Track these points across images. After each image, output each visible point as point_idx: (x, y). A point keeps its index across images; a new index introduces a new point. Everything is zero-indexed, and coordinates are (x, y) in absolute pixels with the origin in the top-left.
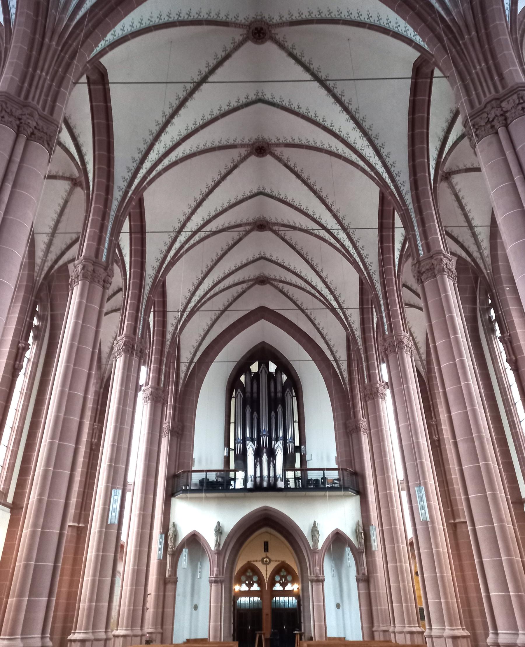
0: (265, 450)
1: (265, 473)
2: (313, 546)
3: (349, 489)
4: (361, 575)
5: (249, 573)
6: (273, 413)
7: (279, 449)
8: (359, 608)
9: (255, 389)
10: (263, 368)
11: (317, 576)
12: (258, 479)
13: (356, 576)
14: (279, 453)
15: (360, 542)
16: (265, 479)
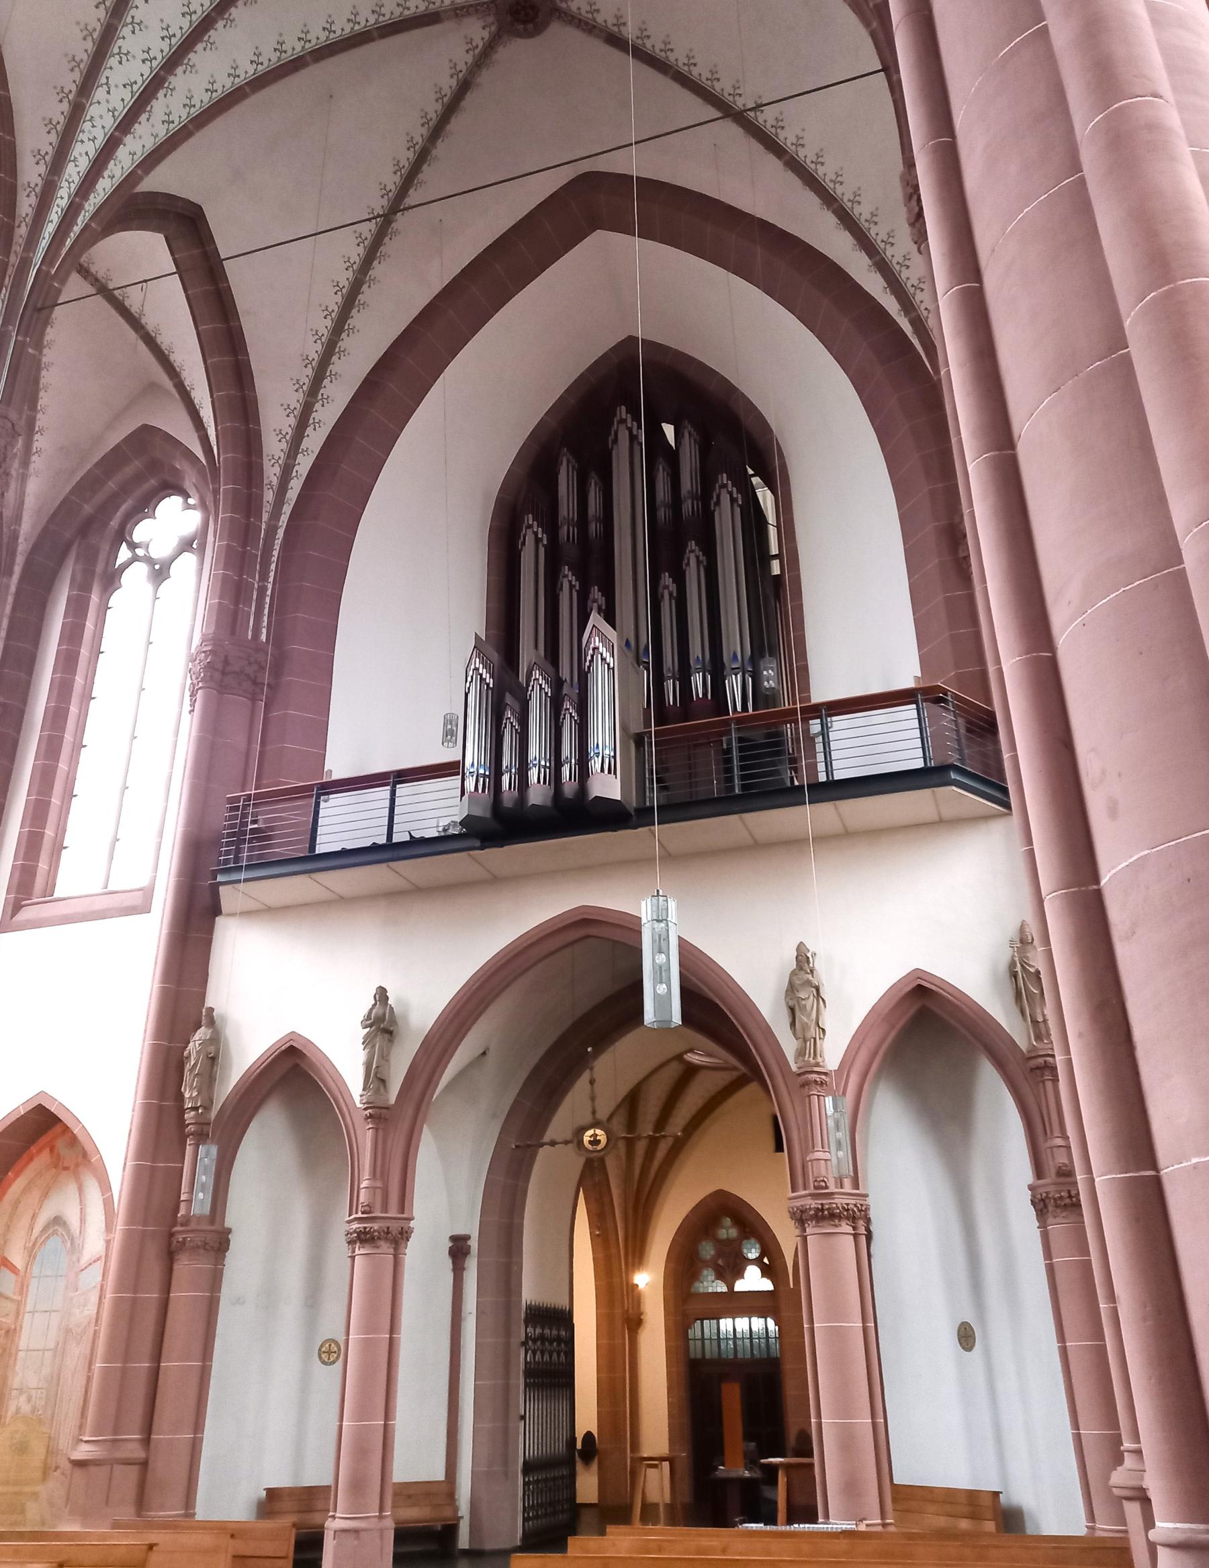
2: (801, 1053)
3: (953, 776)
4: (1051, 1177)
5: (728, 1231)
8: (1055, 1345)
11: (821, 1190)
13: (1031, 1188)
15: (1035, 1022)
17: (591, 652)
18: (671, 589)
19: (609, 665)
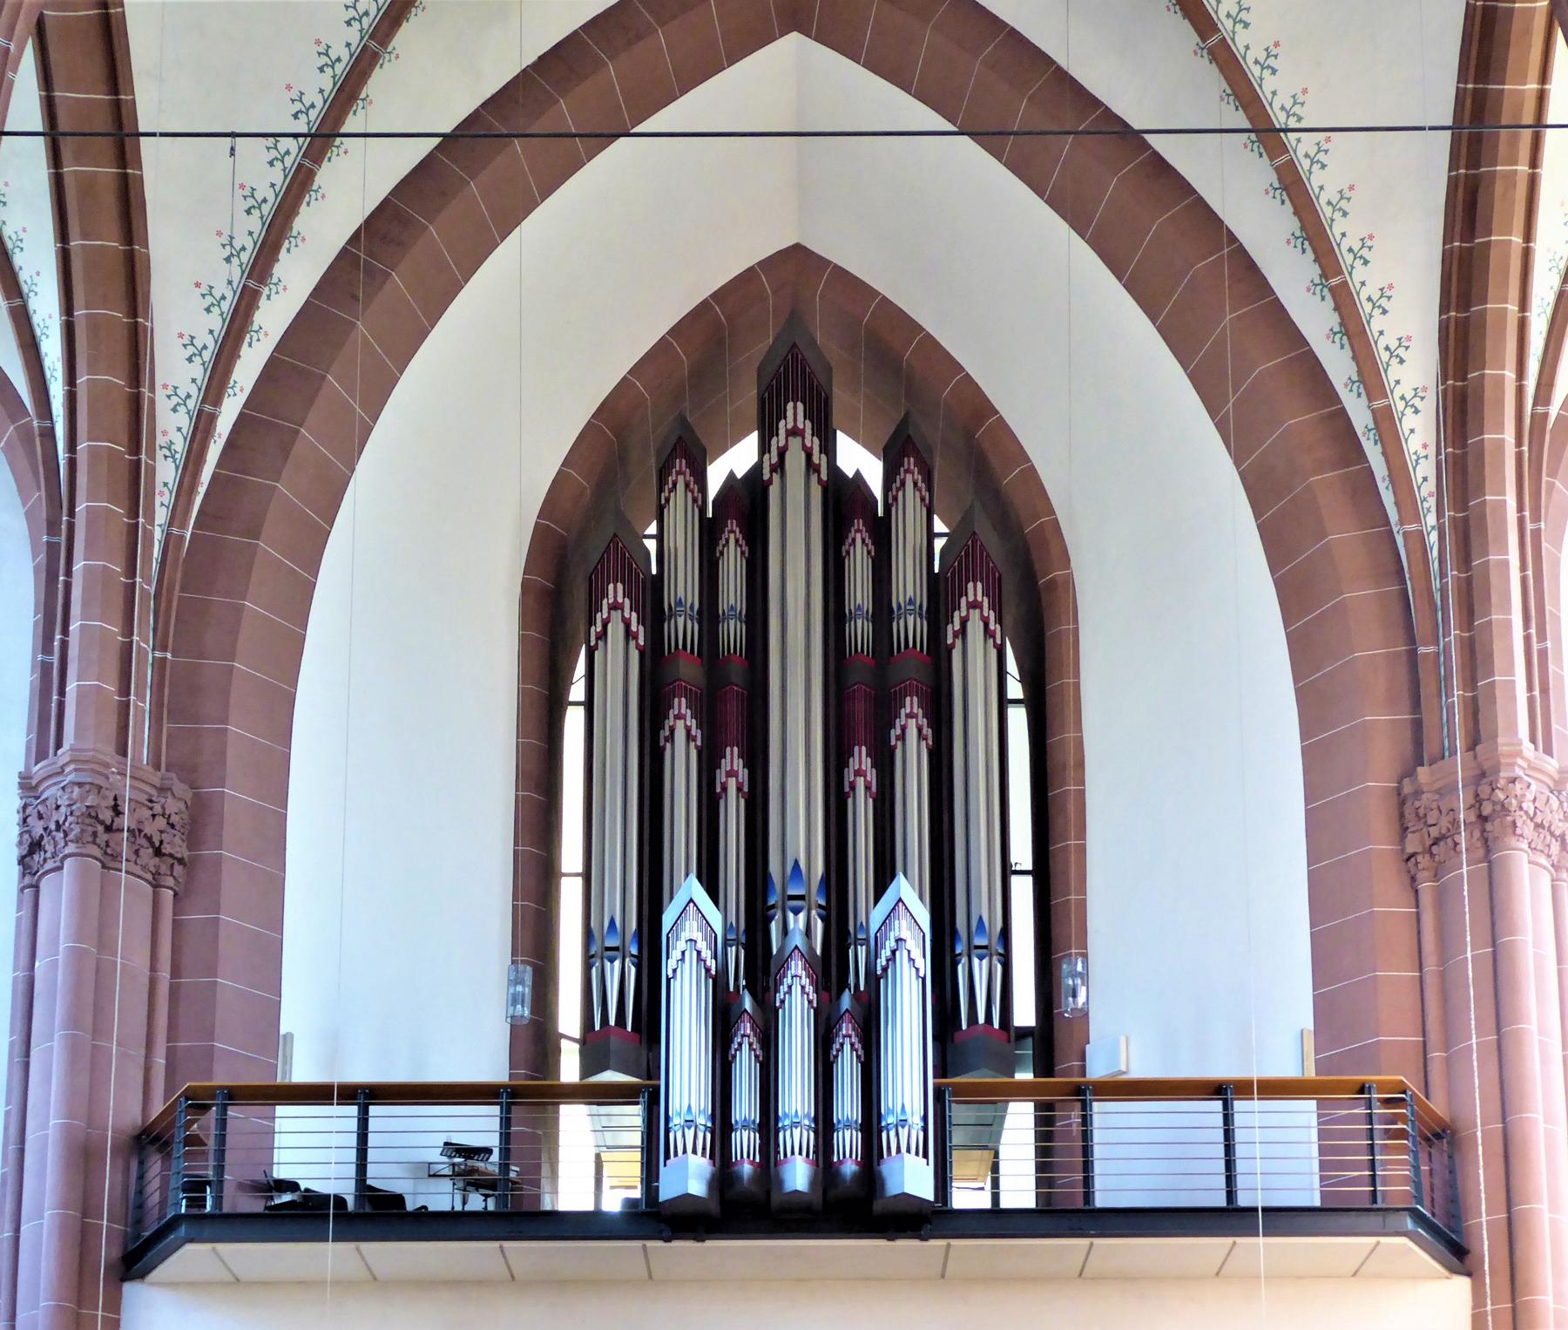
0: (797, 967)
1: (796, 1097)
6: (861, 759)
7: (902, 928)
9: (732, 591)
10: (794, 432)
12: (745, 1142)
14: (902, 957)
16: (797, 1137)
17: (890, 944)
18: (869, 779)
19: (917, 970)
